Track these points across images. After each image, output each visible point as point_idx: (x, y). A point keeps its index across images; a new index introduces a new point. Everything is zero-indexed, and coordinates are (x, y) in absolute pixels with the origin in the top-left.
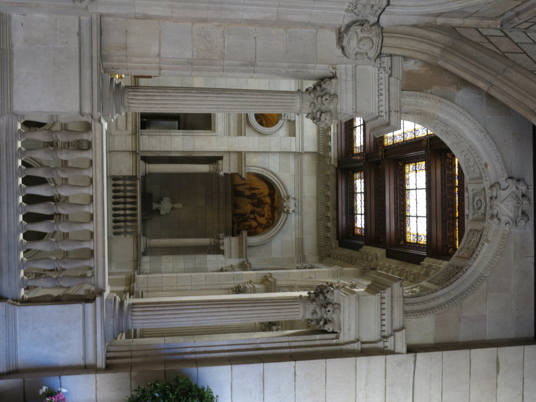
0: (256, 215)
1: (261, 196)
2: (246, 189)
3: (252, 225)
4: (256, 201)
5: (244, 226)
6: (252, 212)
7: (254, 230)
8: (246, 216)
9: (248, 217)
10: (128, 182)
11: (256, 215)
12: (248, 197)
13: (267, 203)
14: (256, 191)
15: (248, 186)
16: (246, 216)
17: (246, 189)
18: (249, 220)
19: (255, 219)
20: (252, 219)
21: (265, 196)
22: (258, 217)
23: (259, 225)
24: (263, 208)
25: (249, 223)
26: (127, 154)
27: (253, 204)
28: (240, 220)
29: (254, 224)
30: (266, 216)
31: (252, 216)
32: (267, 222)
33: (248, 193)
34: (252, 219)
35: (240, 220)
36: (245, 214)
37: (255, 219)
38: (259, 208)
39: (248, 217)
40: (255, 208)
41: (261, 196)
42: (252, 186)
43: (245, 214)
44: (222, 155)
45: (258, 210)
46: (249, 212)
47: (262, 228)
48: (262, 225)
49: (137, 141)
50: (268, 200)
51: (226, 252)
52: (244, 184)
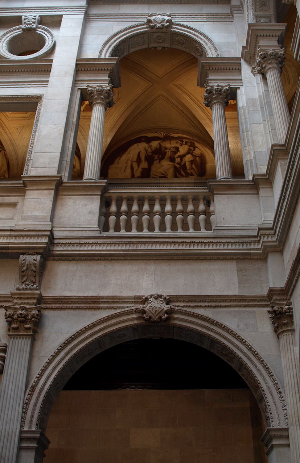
0: (177, 155)
1: (149, 150)
2: (139, 165)
3: (190, 159)
4: (156, 157)
5: (192, 168)
6: (172, 160)
7: (197, 158)
8: (178, 166)
9: (178, 164)
10: (113, 208)
11: (177, 155)
12: (150, 164)
13: (159, 144)
14: (143, 157)
15: (135, 165)
16: (178, 166)
17: (139, 165)
18: (183, 163)
19: (182, 157)
20: (181, 160)
21: (150, 146)
22: (178, 154)
23: (189, 152)
24: (166, 148)
25: (188, 164)
26: (59, 202)
27: (161, 159)
28: (183, 173)
29: (188, 158)
30: (177, 145)
31: (178, 160)
32: (186, 143)
33: (144, 165)
34: (181, 160)
35: (183, 173)
36: (175, 167)
37: (182, 157)
38: (166, 152)
39: (178, 164)
40: (166, 157)
41: (149, 150)
42: (135, 158)
43: (175, 167)
44: (79, 92)
45: (169, 153)
46: (172, 163)
47: (194, 150)
48: (190, 149)
49: (39, 182)
50: (155, 144)
51: (233, 85)
52: (132, 168)
